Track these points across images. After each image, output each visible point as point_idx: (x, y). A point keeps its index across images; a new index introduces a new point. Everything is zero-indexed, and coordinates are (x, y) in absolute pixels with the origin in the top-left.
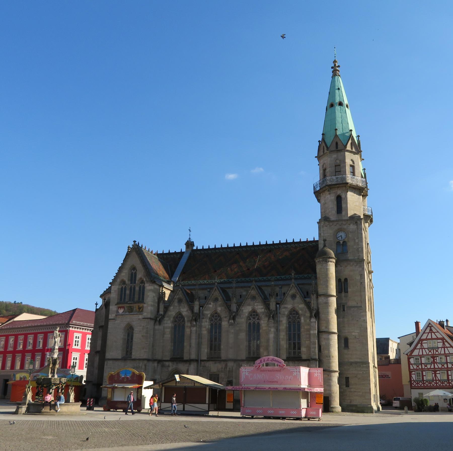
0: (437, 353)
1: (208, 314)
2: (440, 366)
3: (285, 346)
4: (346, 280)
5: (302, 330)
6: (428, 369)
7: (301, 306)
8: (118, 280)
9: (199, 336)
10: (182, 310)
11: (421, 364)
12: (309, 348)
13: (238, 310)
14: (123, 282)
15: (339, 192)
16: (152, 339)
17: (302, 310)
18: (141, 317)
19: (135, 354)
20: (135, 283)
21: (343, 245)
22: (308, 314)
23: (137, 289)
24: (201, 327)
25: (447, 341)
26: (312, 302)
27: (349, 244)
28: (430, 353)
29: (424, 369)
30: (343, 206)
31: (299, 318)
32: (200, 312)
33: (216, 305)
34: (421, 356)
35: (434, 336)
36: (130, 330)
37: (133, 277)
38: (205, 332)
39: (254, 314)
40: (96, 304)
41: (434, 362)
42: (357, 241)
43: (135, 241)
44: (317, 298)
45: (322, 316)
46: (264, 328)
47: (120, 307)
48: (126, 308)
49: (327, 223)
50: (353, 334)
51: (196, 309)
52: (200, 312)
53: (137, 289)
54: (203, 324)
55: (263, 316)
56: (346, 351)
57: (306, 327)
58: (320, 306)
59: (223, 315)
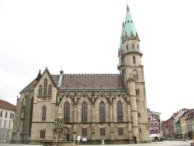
4: (138, 90)
7: (122, 100)
8: (38, 85)
9: (77, 112)
10: (68, 100)
12: (127, 117)
13: (95, 101)
14: (41, 86)
15: (134, 55)
18: (50, 103)
19: (47, 120)
20: (46, 87)
23: (48, 89)
25: (153, 116)
30: (136, 61)
32: (77, 101)
33: (84, 99)
36: (44, 108)
37: (46, 84)
38: (79, 111)
39: (102, 102)
40: (18, 96)
43: (46, 68)
45: (131, 104)
46: (107, 109)
48: (42, 98)
51: (76, 100)
52: (77, 101)
53: (48, 89)
54: (79, 107)
55: (106, 104)
59: (88, 103)
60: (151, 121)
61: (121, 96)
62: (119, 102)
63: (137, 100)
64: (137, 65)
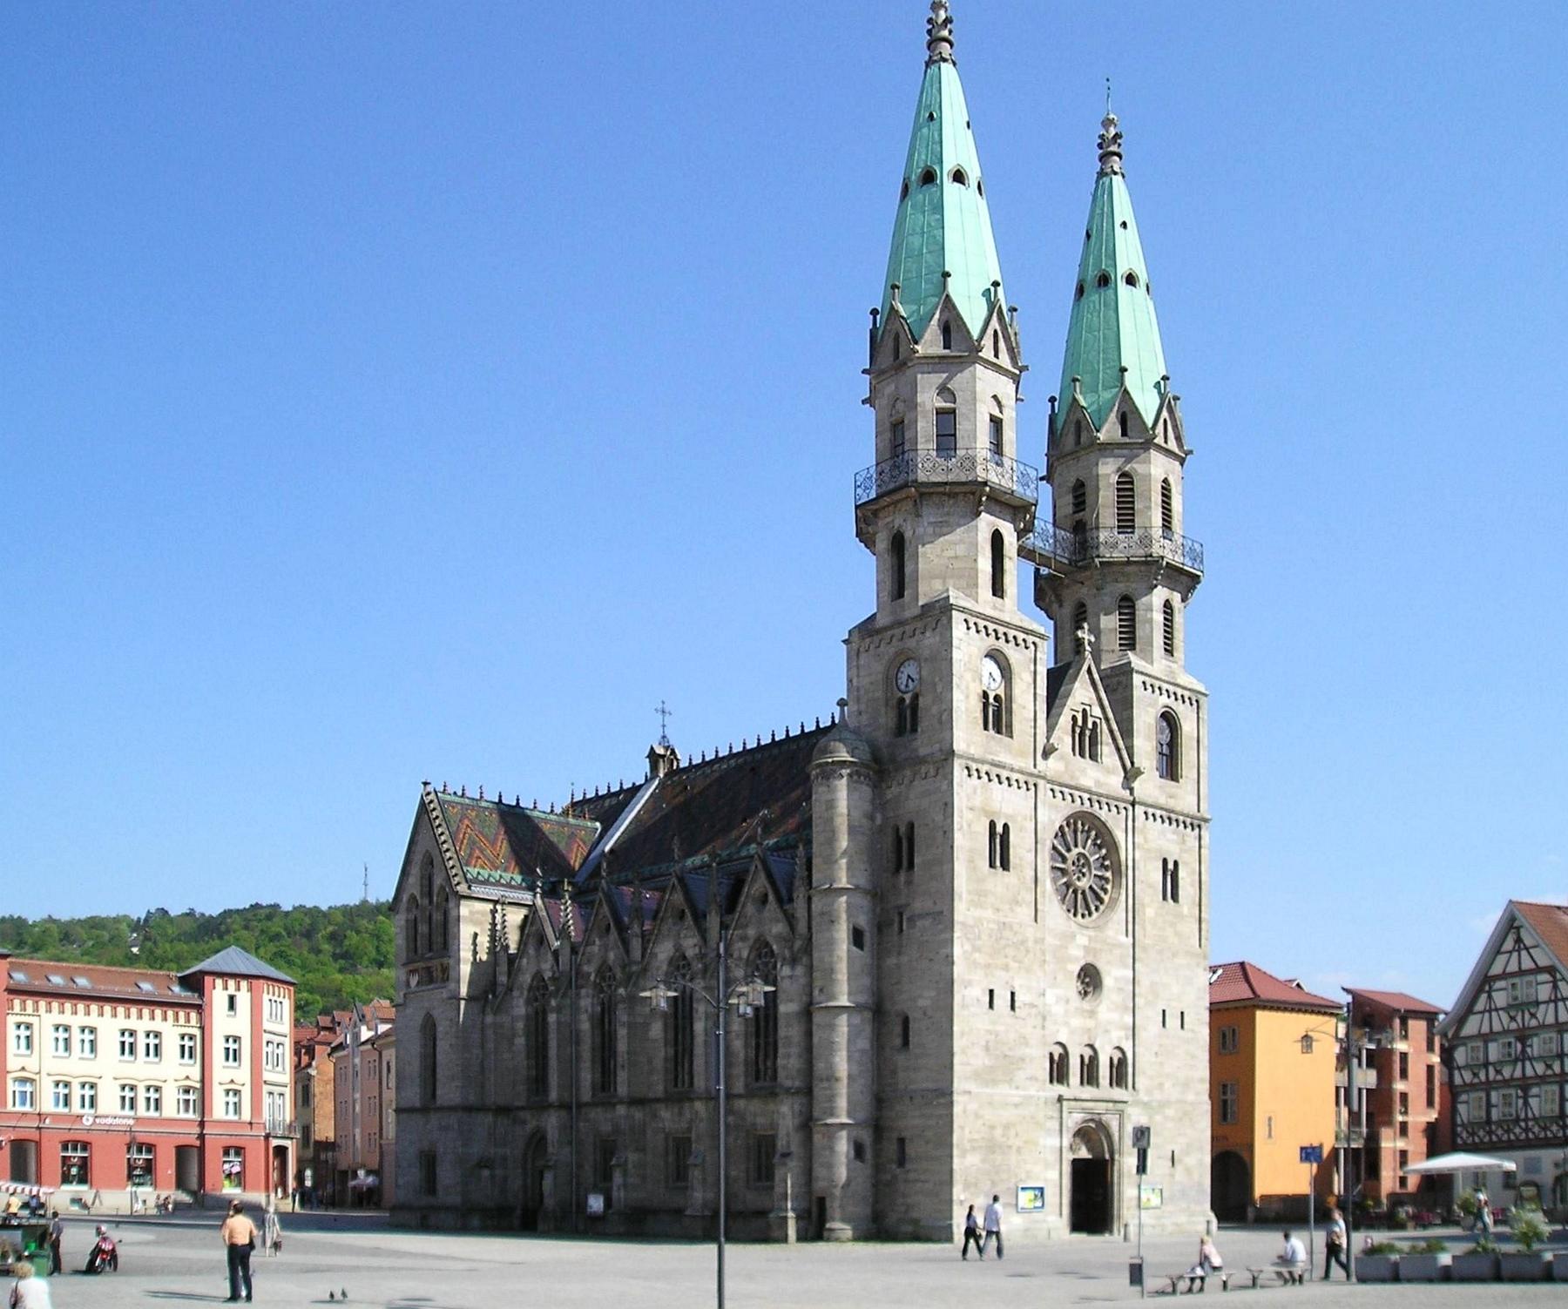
0: (1534, 1023)
1: (589, 974)
2: (1540, 1068)
3: (742, 1055)
4: (911, 826)
6: (1506, 1083)
11: (1486, 1065)
16: (477, 1051)
17: (779, 937)
24: (575, 1009)
28: (1513, 1026)
29: (1495, 1081)
34: (1487, 1038)
35: (1527, 964)
41: (1523, 1058)
47: (412, 972)
50: (921, 1003)
56: (901, 1059)
60: (1543, 1027)
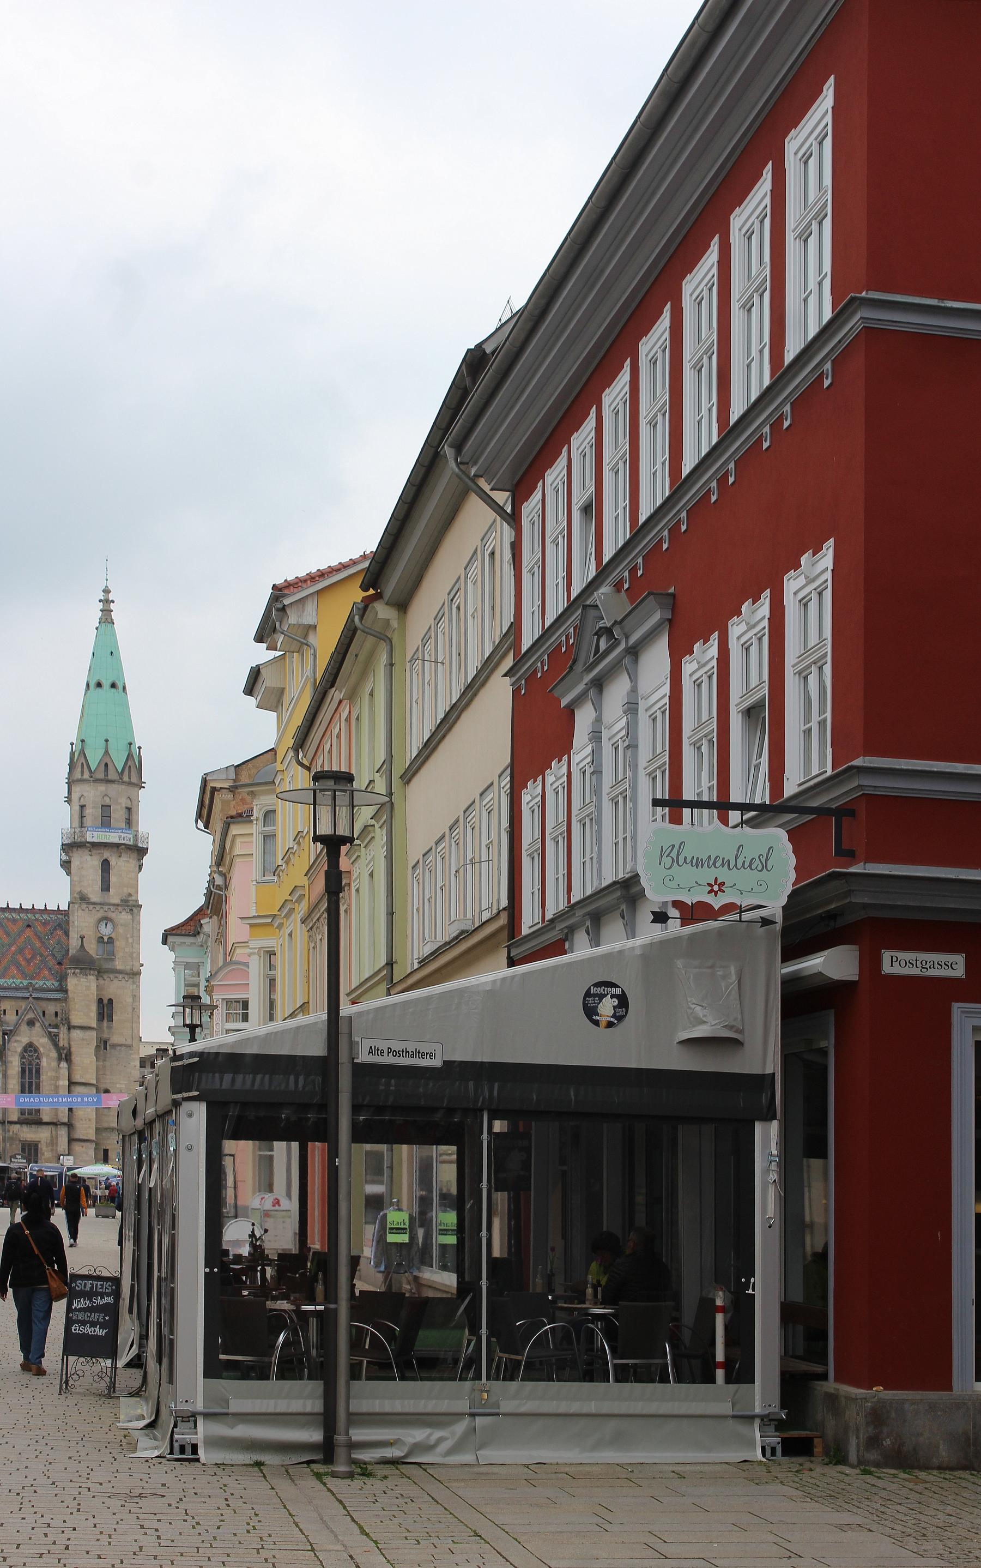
4: (111, 1001)
5: (43, 1077)
7: (43, 1042)
21: (108, 943)
22: (54, 1054)
26: (61, 1036)
27: (117, 944)
30: (113, 879)
31: (38, 1058)
42: (130, 940)
44: (69, 1029)
49: (84, 906)
50: (118, 1086)
57: (49, 1074)
58: (72, 1043)
61: (38, 1024)
62: (30, 1048)
63: (103, 1045)
64: (114, 896)
